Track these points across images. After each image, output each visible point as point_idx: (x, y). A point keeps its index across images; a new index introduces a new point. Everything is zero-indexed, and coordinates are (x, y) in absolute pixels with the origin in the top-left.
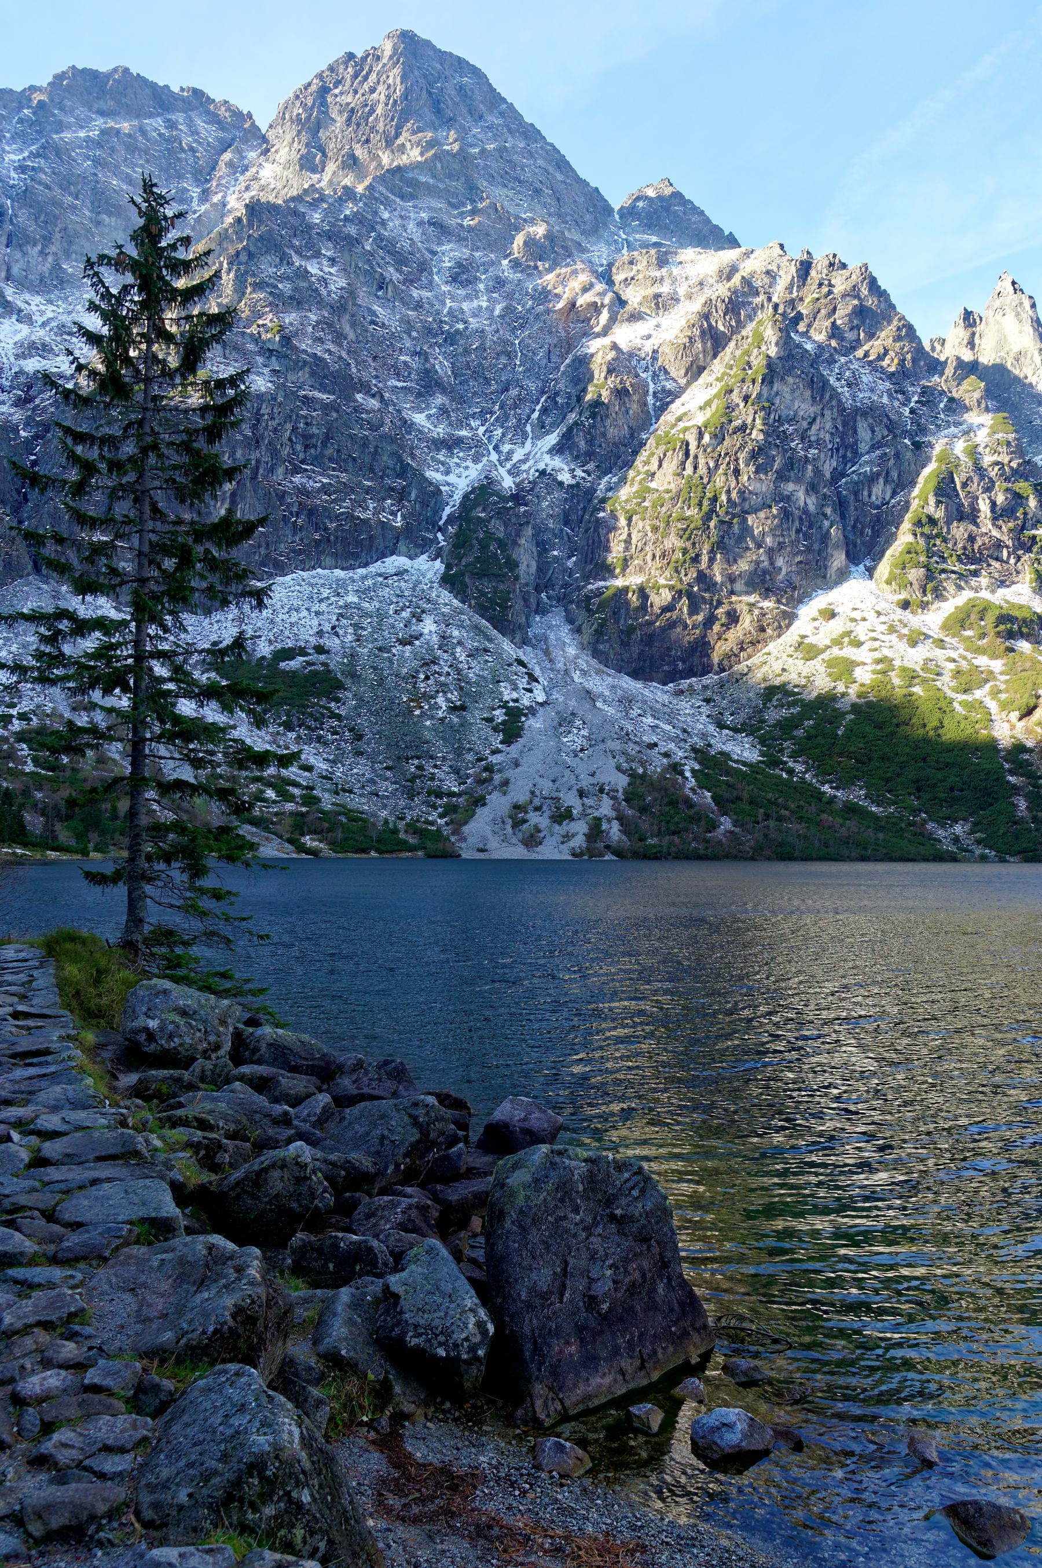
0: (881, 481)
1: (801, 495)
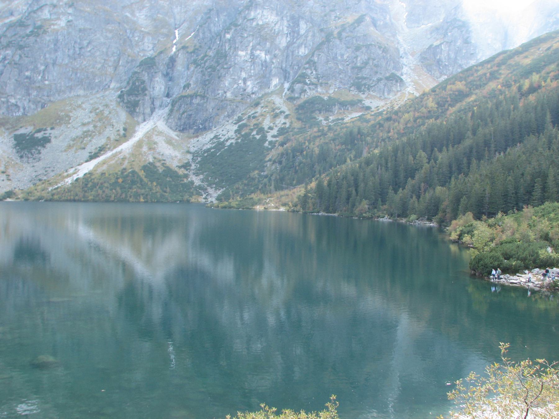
0: (303, 46)
1: (263, 55)
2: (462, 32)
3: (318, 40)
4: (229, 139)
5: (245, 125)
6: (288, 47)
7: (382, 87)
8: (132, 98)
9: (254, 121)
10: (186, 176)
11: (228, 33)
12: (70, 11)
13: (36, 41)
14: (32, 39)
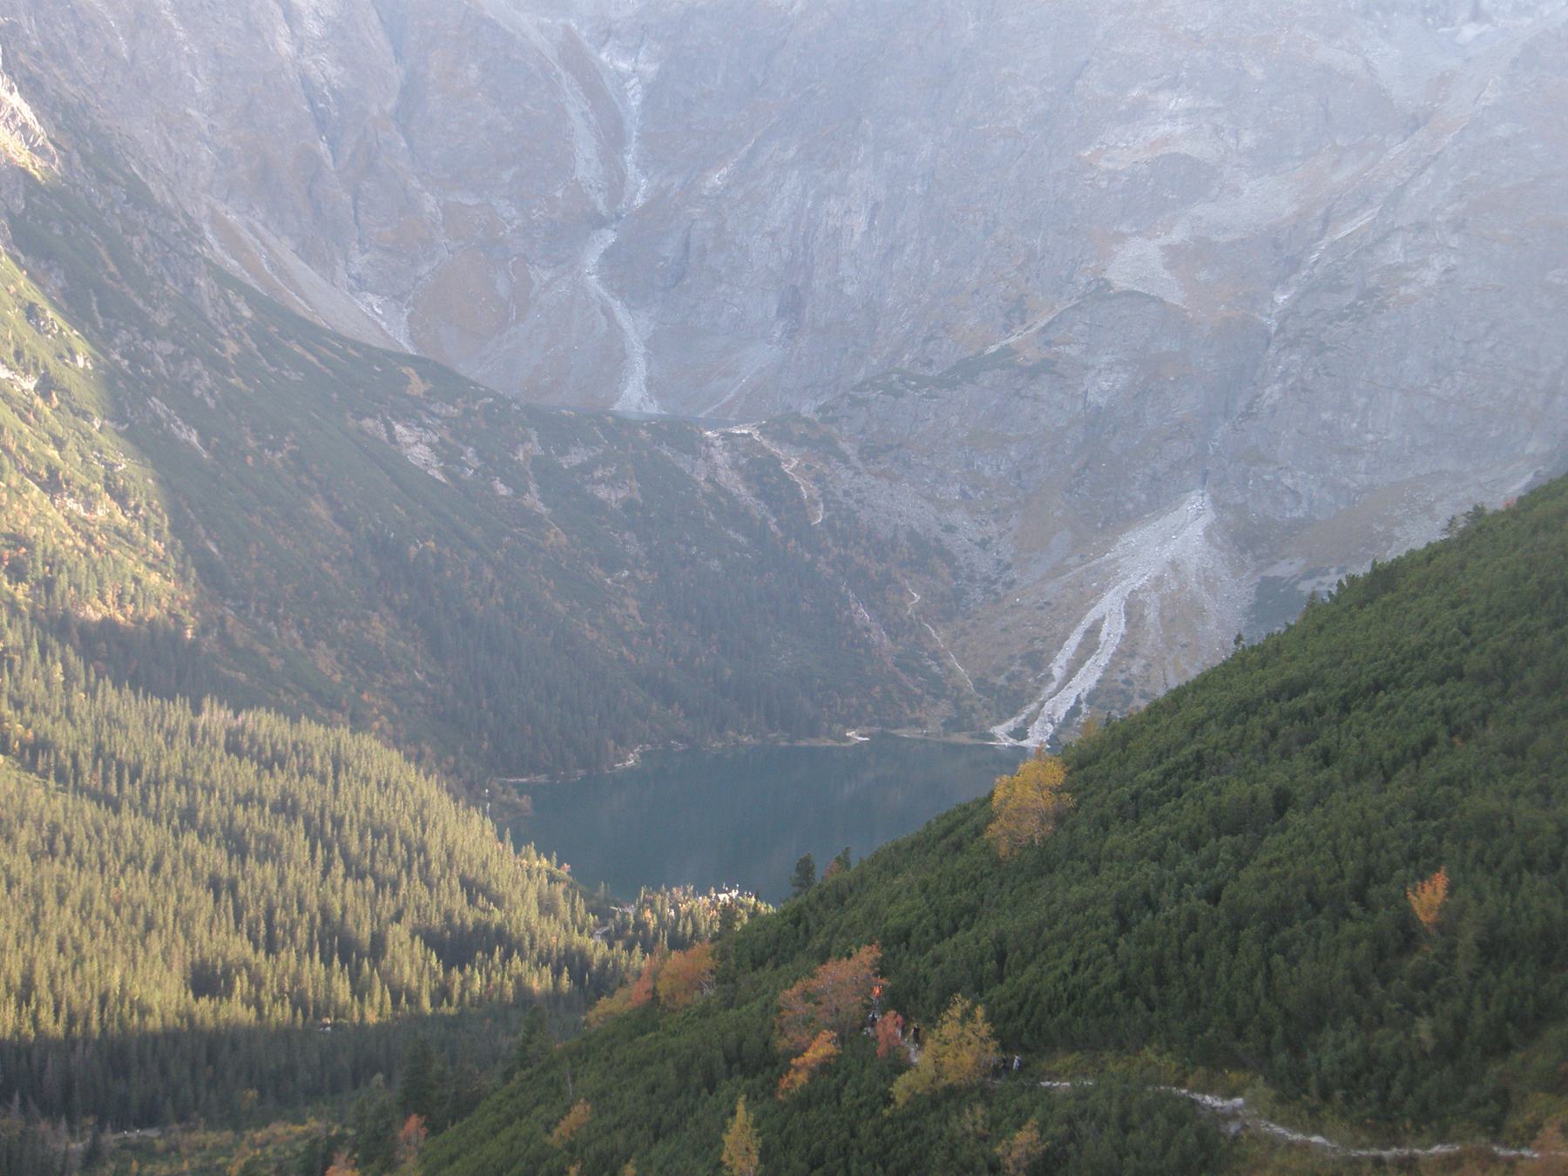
12: (1454, 241)
13: (1355, 332)
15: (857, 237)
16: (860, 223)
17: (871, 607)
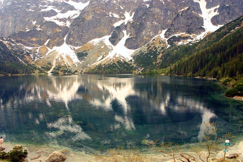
1: (156, 23)
2: (227, 10)
3: (174, 16)
4: (145, 51)
5: (150, 47)
6: (164, 20)
7: (197, 31)
8: (113, 39)
9: (153, 45)
10: (131, 64)
11: (144, 16)
12: (93, 13)
14: (82, 23)
15: (10, 25)
16: (11, 23)
17: (21, 59)
